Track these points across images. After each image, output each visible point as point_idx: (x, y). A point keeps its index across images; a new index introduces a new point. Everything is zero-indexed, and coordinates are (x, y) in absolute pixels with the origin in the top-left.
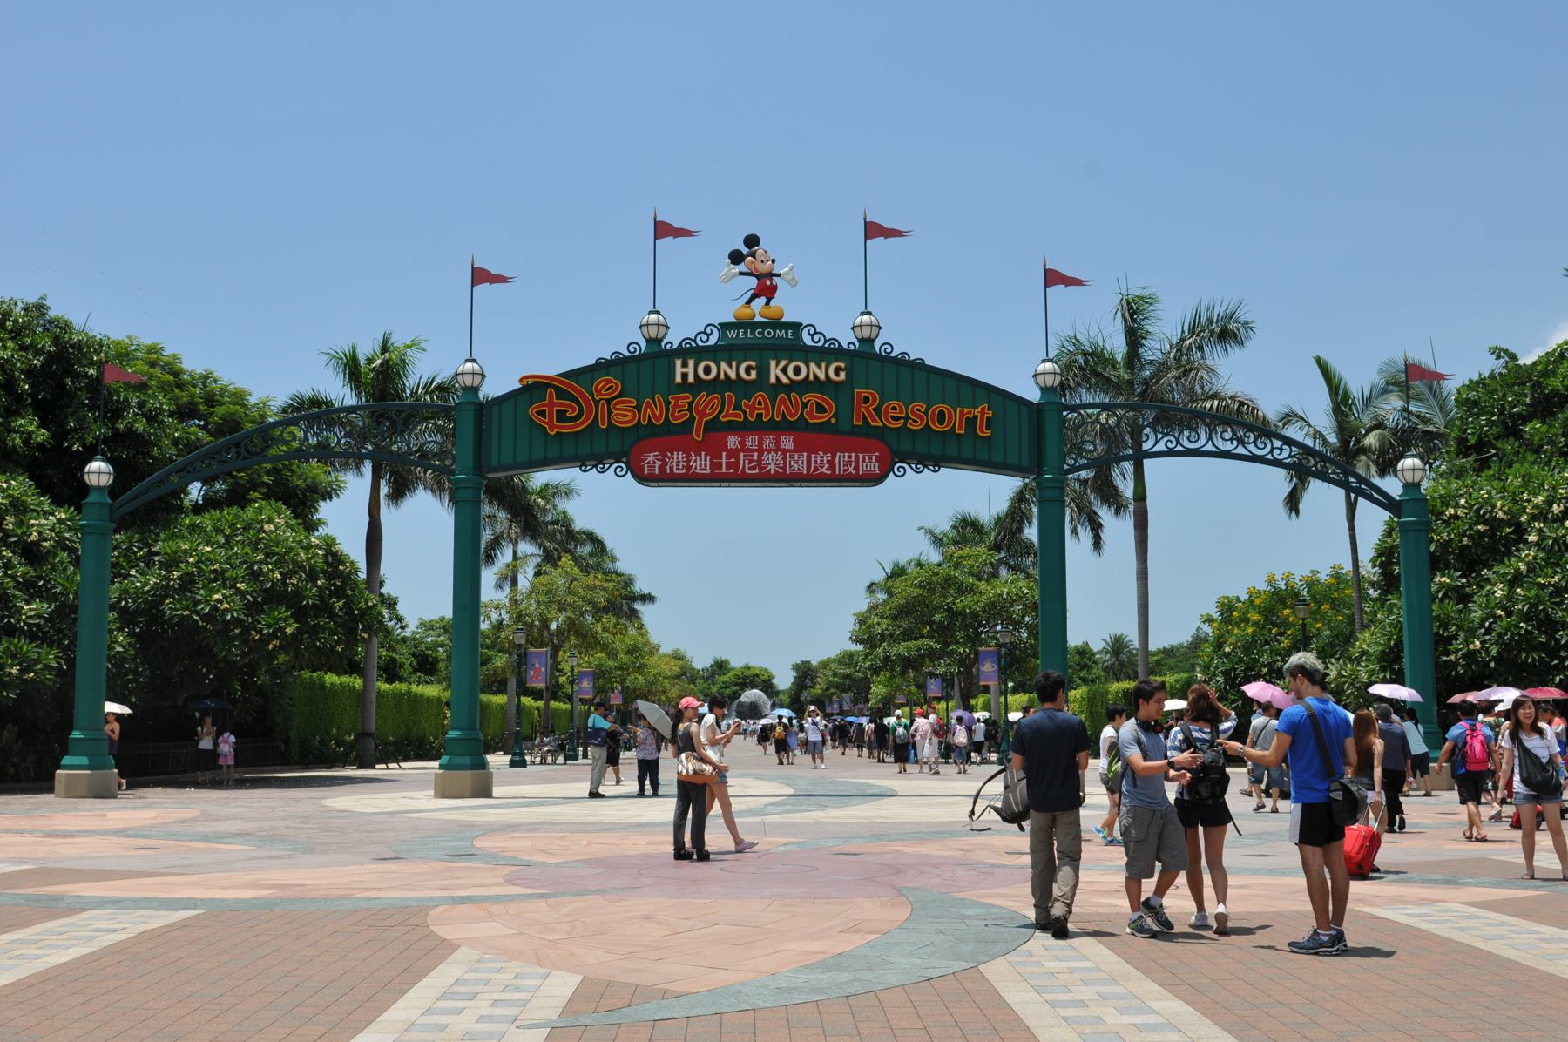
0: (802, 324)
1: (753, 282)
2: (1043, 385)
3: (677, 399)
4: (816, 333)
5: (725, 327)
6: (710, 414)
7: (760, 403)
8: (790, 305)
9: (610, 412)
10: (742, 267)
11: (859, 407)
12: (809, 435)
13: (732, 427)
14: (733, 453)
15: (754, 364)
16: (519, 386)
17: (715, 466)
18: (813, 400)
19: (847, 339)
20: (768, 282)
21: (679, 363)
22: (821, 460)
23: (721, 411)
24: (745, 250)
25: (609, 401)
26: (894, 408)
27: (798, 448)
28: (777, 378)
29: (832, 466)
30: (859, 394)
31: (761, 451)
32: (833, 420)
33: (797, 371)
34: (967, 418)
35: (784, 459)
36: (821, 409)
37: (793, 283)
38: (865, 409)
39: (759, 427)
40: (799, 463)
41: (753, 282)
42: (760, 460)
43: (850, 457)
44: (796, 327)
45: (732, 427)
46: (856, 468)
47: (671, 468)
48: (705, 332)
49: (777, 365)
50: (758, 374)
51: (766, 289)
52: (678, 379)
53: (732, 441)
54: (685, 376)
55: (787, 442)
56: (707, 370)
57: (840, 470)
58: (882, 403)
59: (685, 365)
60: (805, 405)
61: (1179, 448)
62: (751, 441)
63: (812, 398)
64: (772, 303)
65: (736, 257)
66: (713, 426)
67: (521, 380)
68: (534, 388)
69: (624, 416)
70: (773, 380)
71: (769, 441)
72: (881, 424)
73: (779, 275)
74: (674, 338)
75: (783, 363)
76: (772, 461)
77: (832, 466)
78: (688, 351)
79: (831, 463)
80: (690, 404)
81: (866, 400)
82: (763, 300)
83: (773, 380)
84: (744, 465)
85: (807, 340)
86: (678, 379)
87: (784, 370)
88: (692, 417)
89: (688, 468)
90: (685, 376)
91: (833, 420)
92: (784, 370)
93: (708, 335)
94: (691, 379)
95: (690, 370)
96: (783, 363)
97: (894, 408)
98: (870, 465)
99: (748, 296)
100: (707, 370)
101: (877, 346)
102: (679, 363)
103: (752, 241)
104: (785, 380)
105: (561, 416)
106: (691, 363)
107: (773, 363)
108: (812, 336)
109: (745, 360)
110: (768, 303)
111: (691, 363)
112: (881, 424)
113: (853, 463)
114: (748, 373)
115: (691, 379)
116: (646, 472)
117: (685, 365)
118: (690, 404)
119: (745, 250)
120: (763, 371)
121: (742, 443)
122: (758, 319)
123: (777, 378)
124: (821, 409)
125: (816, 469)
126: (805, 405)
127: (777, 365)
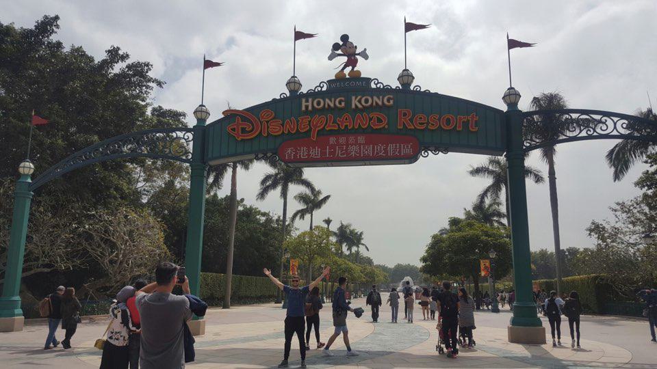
0: (370, 79)
1: (345, 59)
2: (509, 102)
3: (302, 119)
4: (378, 83)
5: (330, 82)
6: (319, 127)
7: (346, 119)
8: (365, 68)
9: (268, 127)
10: (340, 52)
11: (401, 118)
12: (373, 135)
13: (332, 133)
14: (332, 147)
15: (343, 99)
16: (223, 116)
17: (323, 153)
18: (375, 117)
19: (395, 84)
20: (353, 58)
21: (304, 100)
22: (380, 148)
23: (326, 123)
24: (341, 43)
25: (267, 122)
26: (421, 118)
27: (367, 143)
28: (356, 105)
29: (386, 152)
30: (401, 112)
31: (347, 145)
32: (386, 127)
33: (367, 101)
34: (464, 122)
35: (360, 149)
36: (380, 121)
37: (366, 57)
38: (405, 119)
39: (347, 132)
40: (369, 150)
41: (345, 59)
42: (346, 150)
43: (396, 146)
44: (368, 80)
45: (332, 133)
46: (400, 152)
47: (300, 156)
48: (320, 86)
49: (356, 99)
50: (345, 105)
51: (352, 62)
52: (304, 109)
53: (332, 140)
54: (307, 107)
55: (361, 139)
56: (319, 103)
57: (390, 153)
58: (414, 116)
59: (307, 101)
60: (371, 119)
61: (595, 134)
62: (342, 140)
63: (374, 115)
64: (356, 69)
65: (336, 47)
66: (321, 133)
67: (223, 113)
68: (230, 115)
69: (276, 129)
70: (353, 106)
71: (352, 139)
72: (413, 128)
73: (358, 54)
74: (304, 90)
75: (359, 97)
76: (353, 150)
77: (386, 152)
78: (312, 94)
79: (386, 150)
80: (310, 122)
81: (405, 115)
82: (350, 68)
83: (353, 106)
84: (338, 152)
85: (373, 86)
86: (304, 109)
87: (360, 101)
88: (310, 127)
89: (309, 155)
90: (307, 107)
91: (386, 127)
92: (360, 101)
93: (322, 88)
94: (310, 108)
95: (310, 104)
96: (359, 97)
97: (421, 118)
98: (408, 150)
99: (343, 66)
100: (319, 103)
101: (412, 88)
102: (304, 100)
103: (345, 38)
104: (360, 106)
105: (243, 130)
106: (310, 100)
107: (353, 98)
108: (376, 84)
109: (338, 97)
110: (353, 69)
111: (310, 100)
112: (413, 128)
113: (398, 150)
114: (340, 103)
115: (310, 108)
116: (287, 158)
117: (307, 101)
118: (310, 122)
119: (341, 43)
120: (348, 103)
121: (337, 141)
122: (347, 76)
123: (356, 105)
124: (380, 121)
125: (377, 153)
126: (371, 119)
127: (356, 99)
